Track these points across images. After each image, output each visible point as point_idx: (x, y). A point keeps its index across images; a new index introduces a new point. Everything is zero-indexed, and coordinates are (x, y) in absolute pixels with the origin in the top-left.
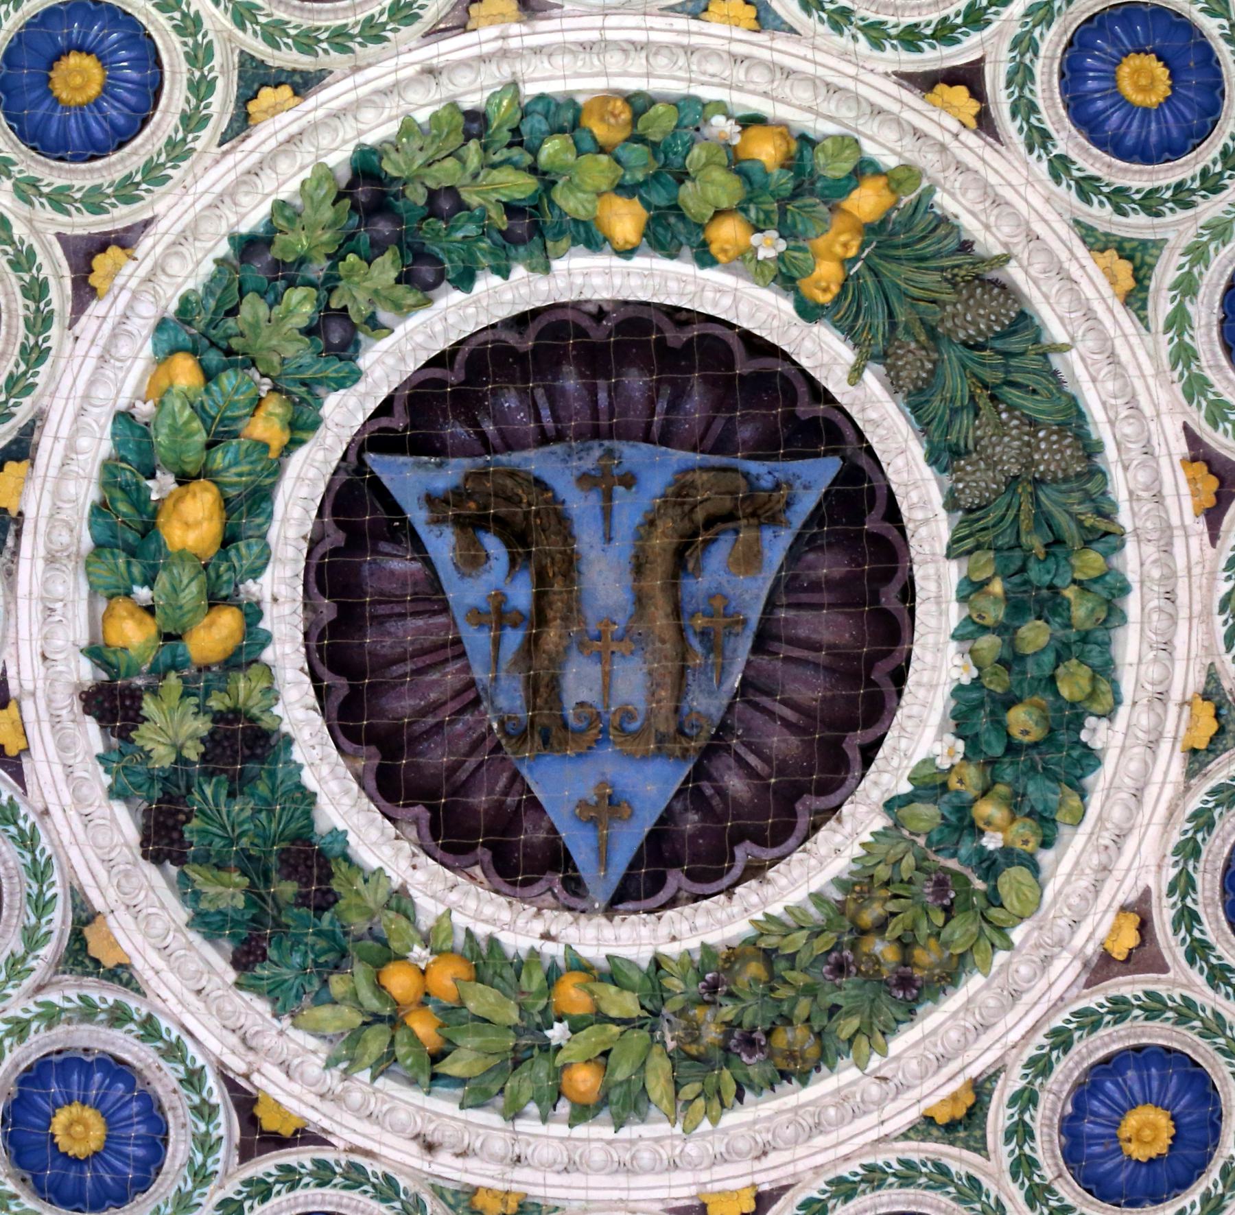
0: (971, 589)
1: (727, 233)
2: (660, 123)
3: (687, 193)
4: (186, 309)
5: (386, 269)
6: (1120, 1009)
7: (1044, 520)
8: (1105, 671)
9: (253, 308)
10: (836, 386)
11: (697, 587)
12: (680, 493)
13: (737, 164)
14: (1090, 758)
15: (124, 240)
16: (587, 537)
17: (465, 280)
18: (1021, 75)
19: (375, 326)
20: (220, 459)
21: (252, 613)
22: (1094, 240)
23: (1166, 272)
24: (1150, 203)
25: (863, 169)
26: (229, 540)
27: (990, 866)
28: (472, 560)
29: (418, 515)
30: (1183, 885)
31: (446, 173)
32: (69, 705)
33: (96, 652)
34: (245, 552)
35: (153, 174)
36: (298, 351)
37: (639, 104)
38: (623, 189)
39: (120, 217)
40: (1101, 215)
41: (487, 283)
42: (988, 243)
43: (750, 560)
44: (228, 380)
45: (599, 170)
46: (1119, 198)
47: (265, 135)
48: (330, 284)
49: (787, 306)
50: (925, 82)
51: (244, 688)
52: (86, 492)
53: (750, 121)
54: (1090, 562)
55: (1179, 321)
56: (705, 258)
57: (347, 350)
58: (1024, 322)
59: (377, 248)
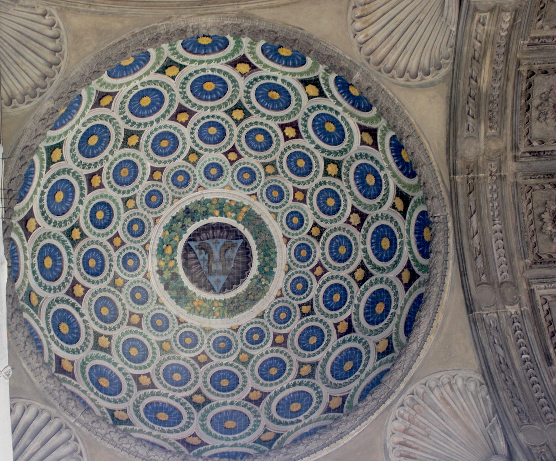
0: (259, 254)
1: (229, 213)
2: (220, 201)
3: (224, 209)
4: (167, 226)
5: (190, 219)
6: (279, 301)
7: (267, 246)
8: (275, 262)
9: (174, 225)
10: (242, 231)
11: (227, 256)
12: (224, 245)
13: (230, 205)
14: (274, 273)
15: (159, 217)
16: (214, 250)
17: (199, 221)
18: (261, 194)
19: (189, 227)
20: (171, 243)
21: (176, 261)
22: (271, 213)
23: (279, 215)
24: (277, 208)
25: (244, 206)
26: (173, 252)
27: (263, 286)
28: (201, 254)
29: (194, 248)
30: (285, 287)
31: (195, 209)
32: (155, 273)
33: (158, 266)
34: (175, 253)
35: (162, 210)
36: (180, 230)
37: (218, 199)
38: (217, 209)
39: (158, 215)
40: (271, 210)
41: (201, 221)
42: (259, 213)
43: (233, 252)
44: (172, 234)
45: (214, 207)
46: (273, 207)
47: (175, 204)
48: (183, 221)
49: (235, 222)
50: (251, 195)
51: (175, 270)
52: (156, 247)
53: (231, 201)
54: (272, 250)
55: (281, 221)
56: (226, 217)
57: (185, 229)
58: (263, 222)
59: (189, 217)
